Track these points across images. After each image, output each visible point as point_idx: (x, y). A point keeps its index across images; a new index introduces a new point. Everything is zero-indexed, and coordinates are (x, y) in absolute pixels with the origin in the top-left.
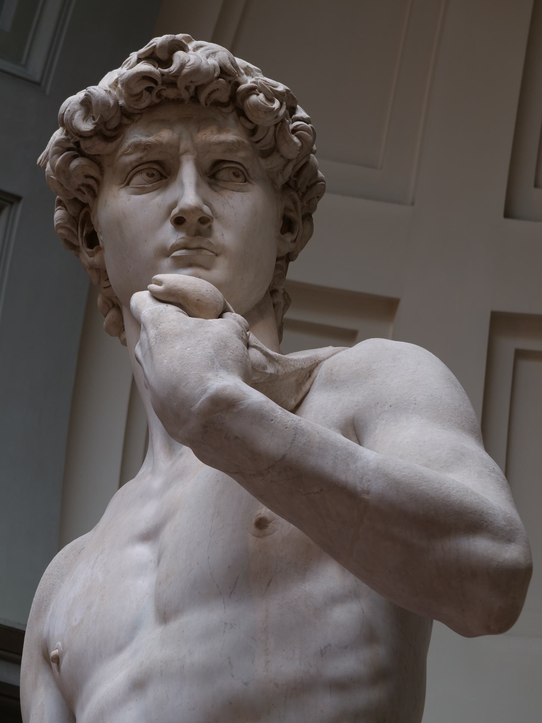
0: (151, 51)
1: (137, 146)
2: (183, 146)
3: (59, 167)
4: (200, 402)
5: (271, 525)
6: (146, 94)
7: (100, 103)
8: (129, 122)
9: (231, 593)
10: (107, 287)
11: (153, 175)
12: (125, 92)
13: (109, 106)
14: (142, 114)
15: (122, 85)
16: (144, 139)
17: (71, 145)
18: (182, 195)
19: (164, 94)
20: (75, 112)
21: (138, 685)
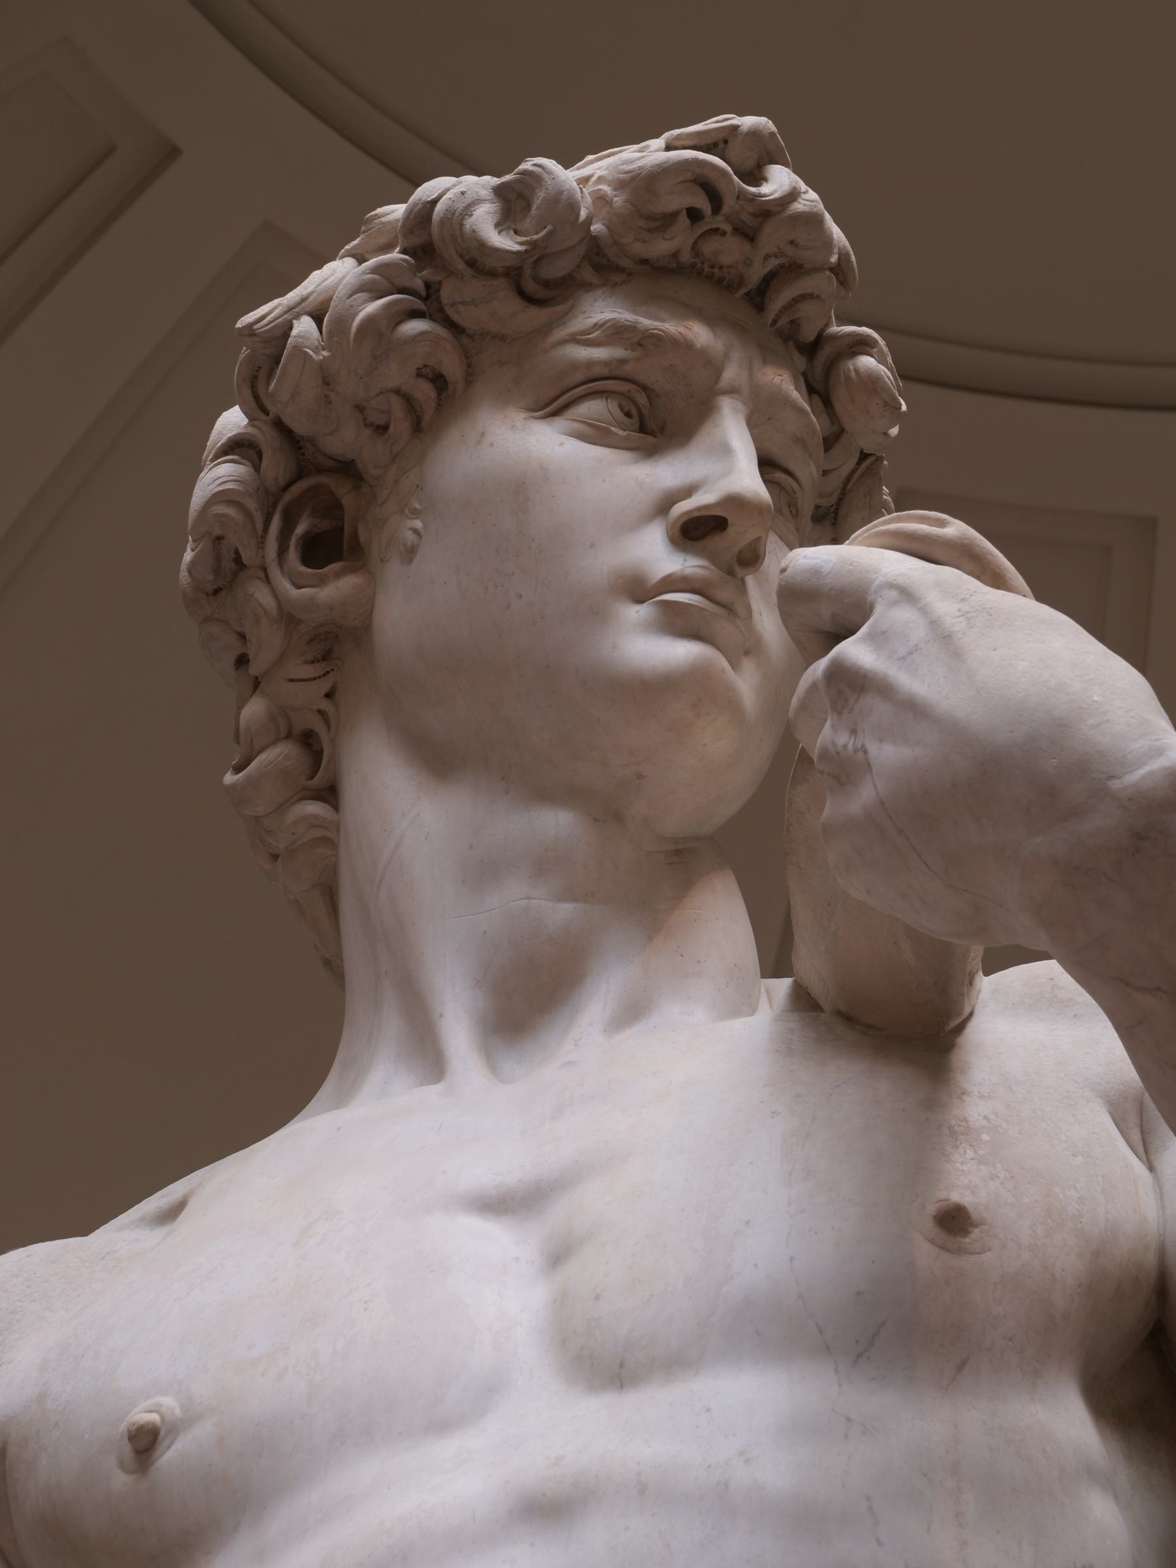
0: (723, 135)
2: (731, 373)
3: (370, 320)
4: (1142, 772)
5: (975, 1233)
6: (684, 220)
7: (564, 197)
8: (595, 280)
9: (860, 1355)
10: (298, 680)
11: (628, 415)
12: (627, 201)
13: (578, 215)
14: (630, 274)
16: (646, 322)
17: (418, 284)
18: (728, 472)
19: (710, 247)
20: (477, 202)
21: (547, 1509)
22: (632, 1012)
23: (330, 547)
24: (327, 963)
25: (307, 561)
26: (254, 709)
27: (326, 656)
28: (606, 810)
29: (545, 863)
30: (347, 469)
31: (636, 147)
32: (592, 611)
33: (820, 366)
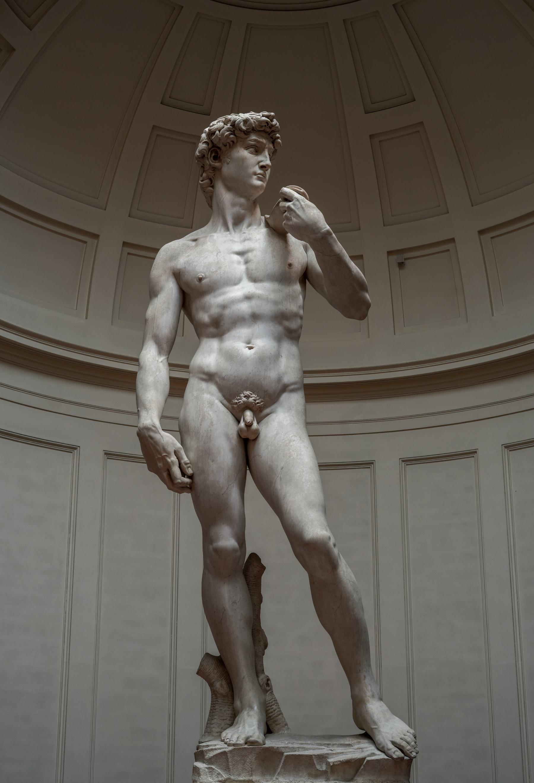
1: (255, 140)
2: (267, 146)
3: (227, 135)
15: (257, 121)
18: (267, 160)
21: (248, 298)
22: (250, 225)
23: (216, 158)
24: (208, 204)
25: (214, 159)
26: (204, 175)
27: (214, 170)
28: (248, 198)
29: (241, 205)
30: (219, 148)
31: (258, 114)
32: (251, 177)
33: (274, 141)
